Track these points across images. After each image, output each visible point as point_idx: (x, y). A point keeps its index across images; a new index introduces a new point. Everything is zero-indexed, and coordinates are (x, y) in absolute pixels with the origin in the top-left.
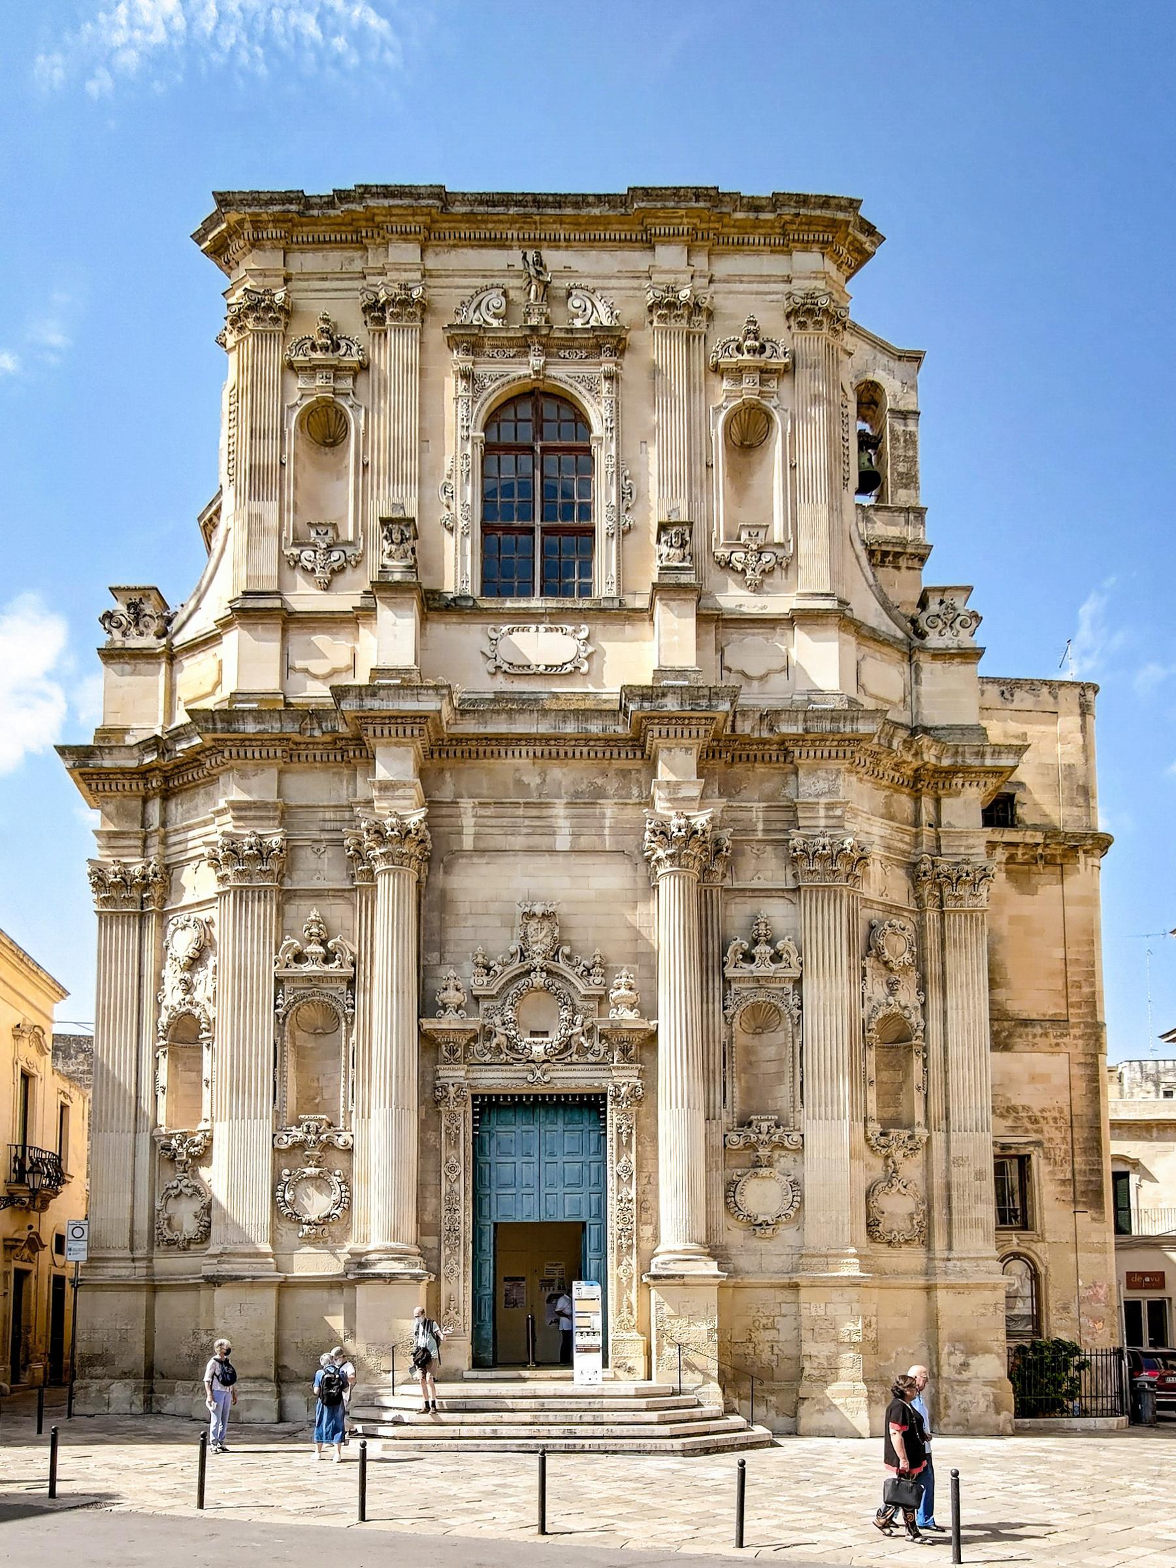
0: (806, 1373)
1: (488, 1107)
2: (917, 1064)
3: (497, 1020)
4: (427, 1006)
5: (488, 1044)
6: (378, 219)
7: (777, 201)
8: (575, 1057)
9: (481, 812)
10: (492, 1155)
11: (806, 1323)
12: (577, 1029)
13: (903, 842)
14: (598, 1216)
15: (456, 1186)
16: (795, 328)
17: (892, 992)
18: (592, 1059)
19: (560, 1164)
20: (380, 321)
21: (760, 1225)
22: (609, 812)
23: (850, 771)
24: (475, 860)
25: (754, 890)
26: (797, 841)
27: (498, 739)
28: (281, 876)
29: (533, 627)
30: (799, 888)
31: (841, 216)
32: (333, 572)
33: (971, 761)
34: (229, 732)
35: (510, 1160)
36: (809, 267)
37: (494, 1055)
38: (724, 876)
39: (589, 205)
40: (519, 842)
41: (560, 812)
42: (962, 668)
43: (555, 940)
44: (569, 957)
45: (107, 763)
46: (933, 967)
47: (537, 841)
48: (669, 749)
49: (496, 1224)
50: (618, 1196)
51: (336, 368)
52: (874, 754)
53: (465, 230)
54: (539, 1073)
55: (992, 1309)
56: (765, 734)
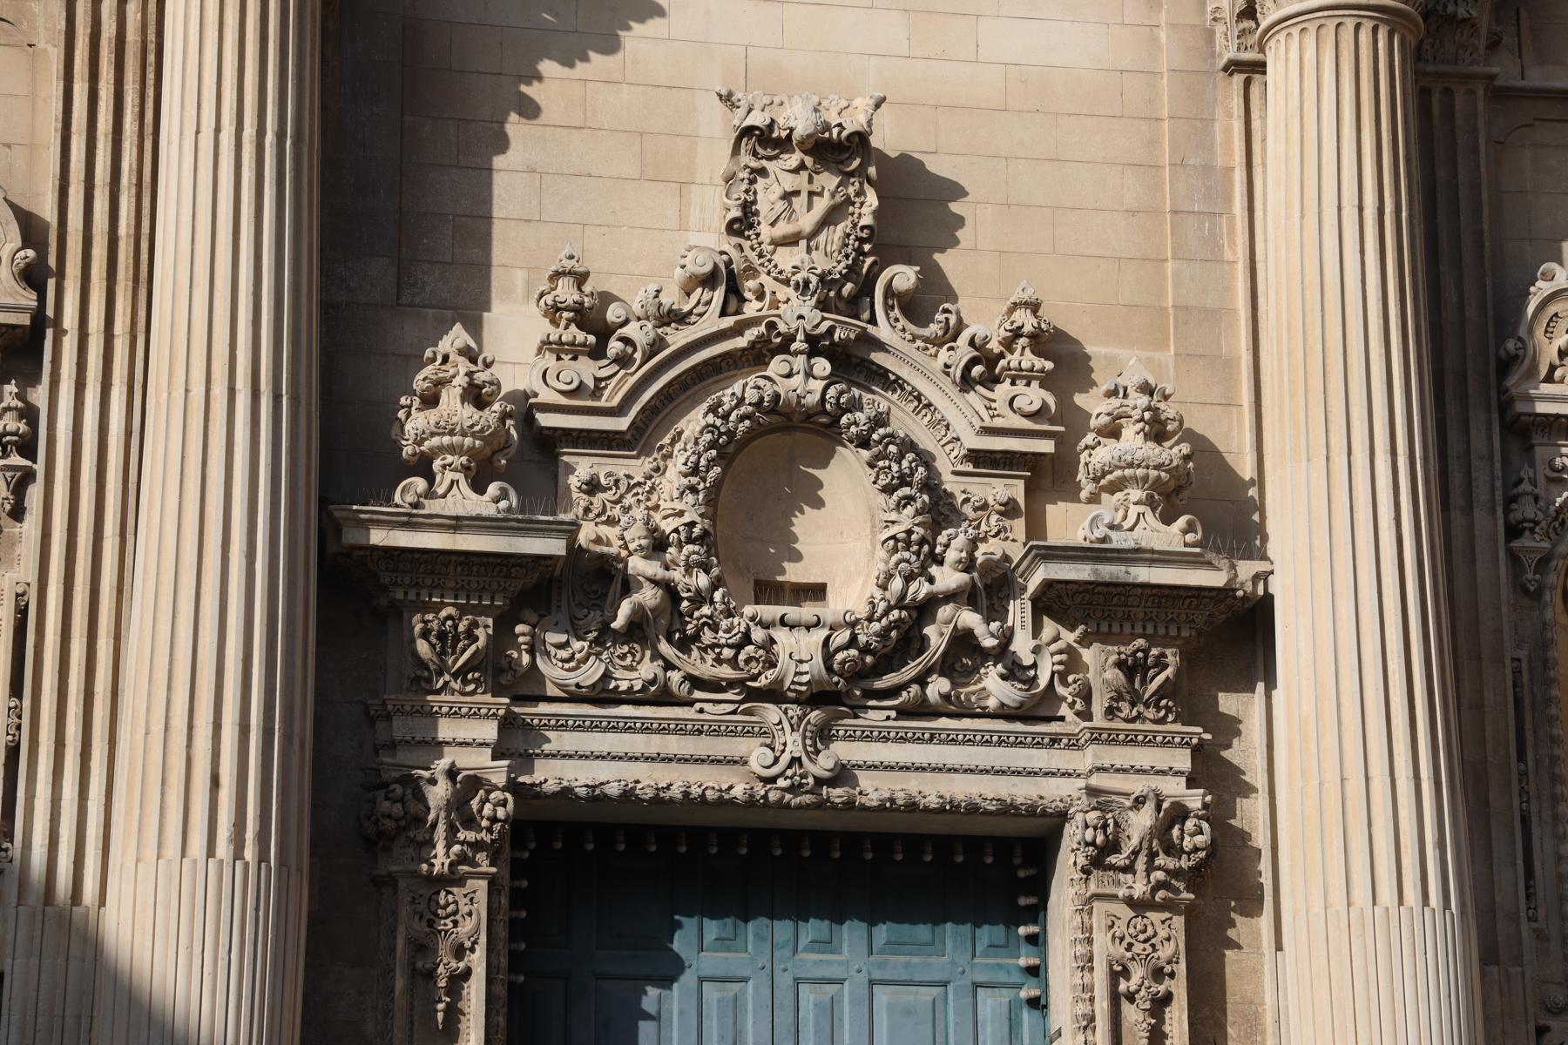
12: (948, 578)
38: (1494, 45)
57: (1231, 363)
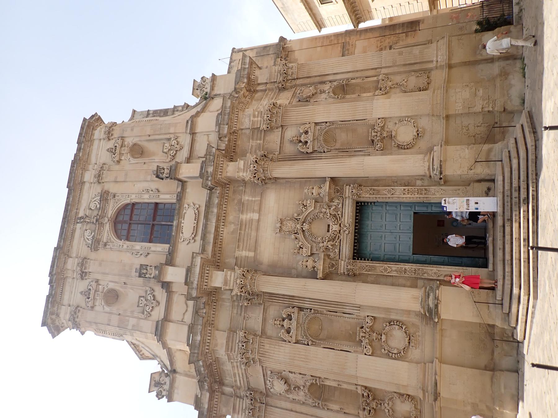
0: (491, 109)
1: (358, 253)
2: (353, 81)
3: (321, 245)
4: (313, 275)
5: (331, 250)
6: (59, 271)
7: (78, 143)
8: (339, 212)
9: (241, 247)
10: (381, 254)
11: (466, 111)
13: (271, 94)
14: (411, 207)
15: (394, 269)
16: (113, 137)
17: (324, 92)
18: (340, 205)
19: (386, 223)
20: (86, 273)
21: (418, 134)
22: (247, 198)
23: (244, 111)
24: (258, 252)
25: (281, 143)
26: (264, 127)
27: (215, 239)
28: (255, 335)
29: (182, 225)
30: (282, 126)
31: (87, 124)
32: (154, 300)
33: (246, 72)
34: (199, 348)
35: (383, 245)
36: (99, 133)
37: (336, 248)
39: (69, 201)
40: (253, 234)
41: (245, 217)
42: (217, 80)
43: (291, 220)
44: (298, 215)
45: (206, 406)
46: (317, 79)
47: (254, 227)
48: (227, 172)
49: (413, 254)
50: (400, 194)
51: (96, 291)
52: (239, 103)
53: (68, 243)
54: (345, 229)
55: (461, 41)
56: (227, 139)
57: (306, 181)
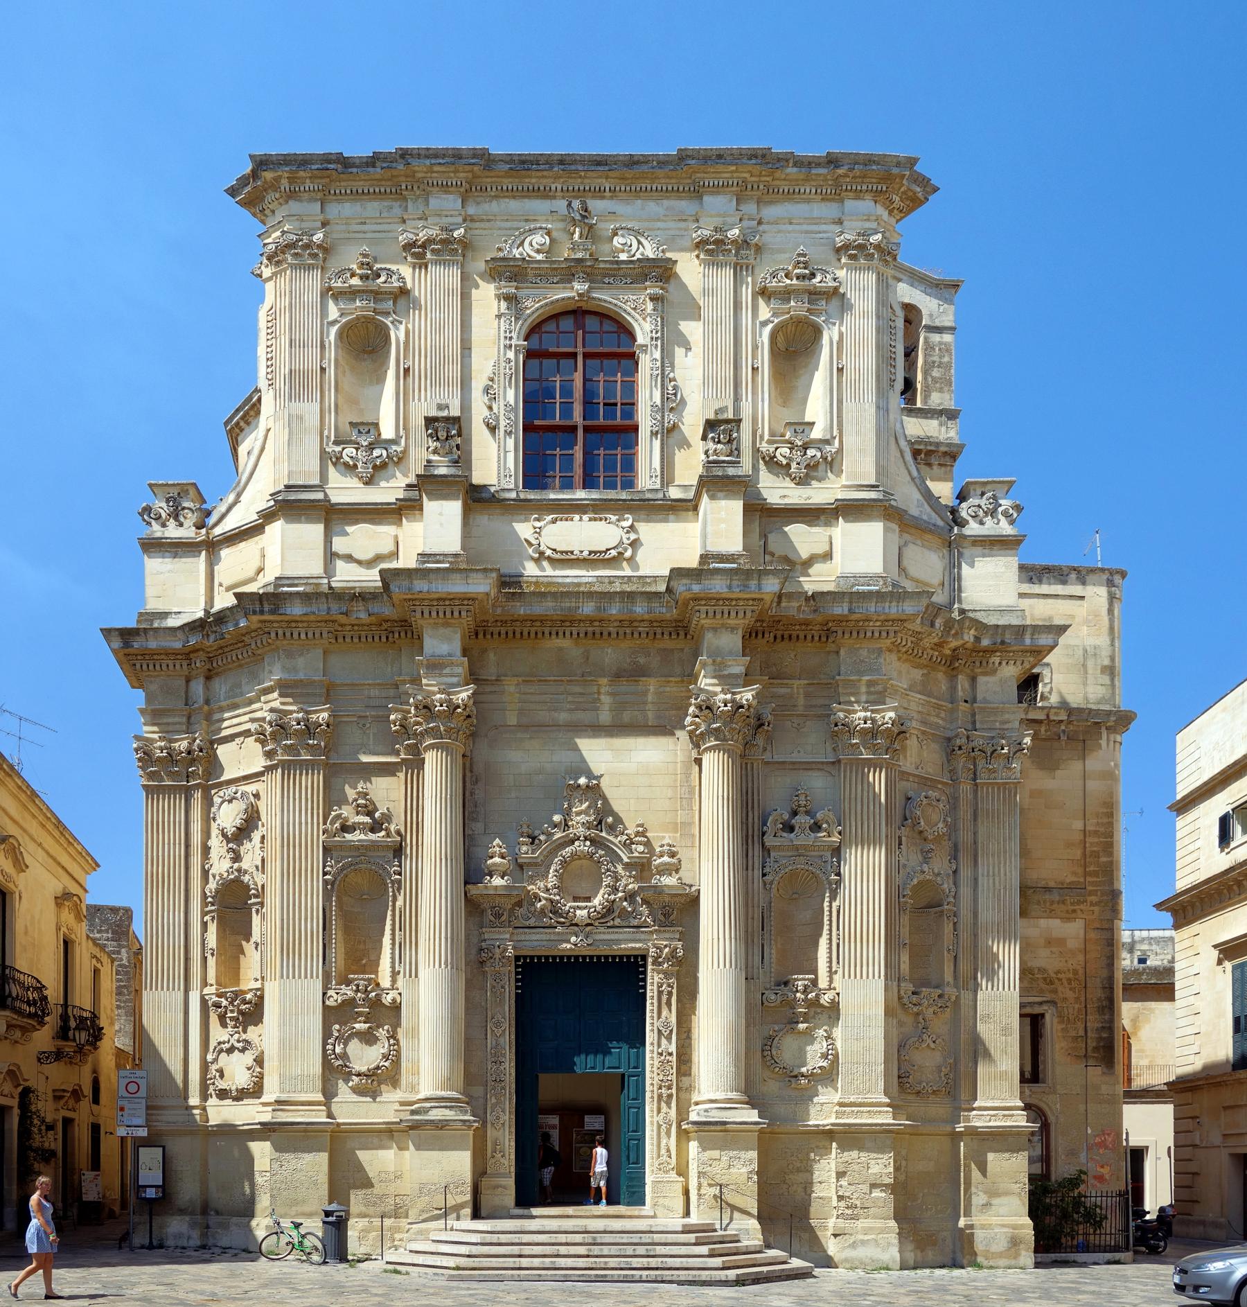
2: (948, 928)
15: (501, 1040)
17: (926, 860)
25: (794, 763)
30: (839, 761)
46: (964, 837)
